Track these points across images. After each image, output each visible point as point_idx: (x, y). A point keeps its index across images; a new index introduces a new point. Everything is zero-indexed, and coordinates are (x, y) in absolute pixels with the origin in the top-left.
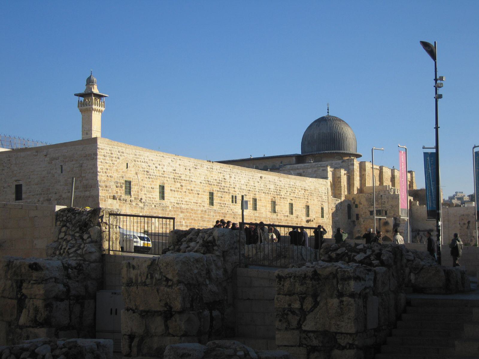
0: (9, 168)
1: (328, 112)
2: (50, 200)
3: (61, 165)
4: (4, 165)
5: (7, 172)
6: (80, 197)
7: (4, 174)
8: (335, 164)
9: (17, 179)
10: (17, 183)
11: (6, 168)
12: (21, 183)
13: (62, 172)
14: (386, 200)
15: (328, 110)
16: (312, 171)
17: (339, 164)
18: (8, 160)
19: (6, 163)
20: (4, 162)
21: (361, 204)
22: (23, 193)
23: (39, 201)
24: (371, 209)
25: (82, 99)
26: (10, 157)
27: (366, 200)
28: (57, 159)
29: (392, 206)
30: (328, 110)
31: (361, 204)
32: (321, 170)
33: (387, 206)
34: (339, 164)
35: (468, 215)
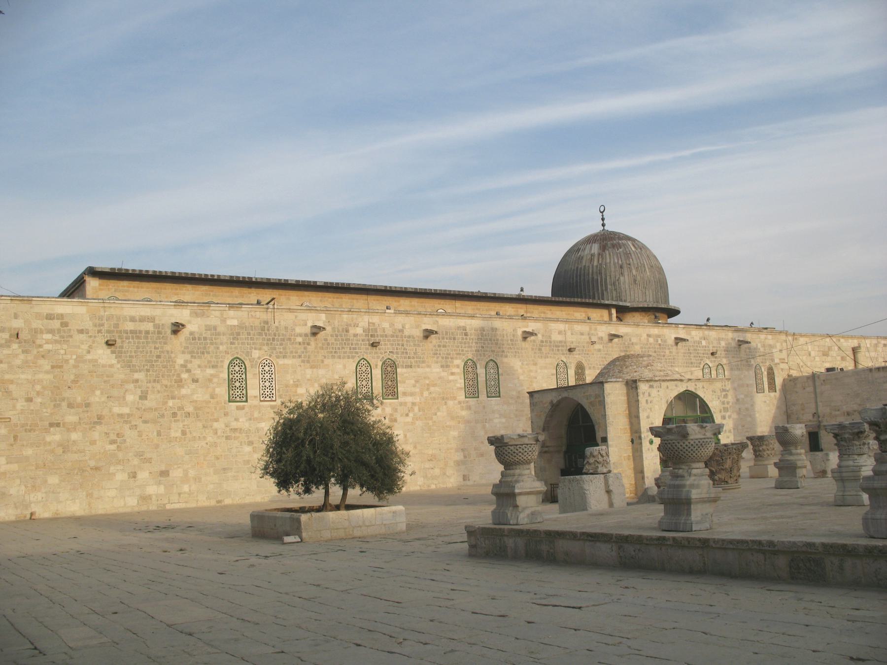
1: (603, 225)
15: (603, 219)
30: (603, 219)
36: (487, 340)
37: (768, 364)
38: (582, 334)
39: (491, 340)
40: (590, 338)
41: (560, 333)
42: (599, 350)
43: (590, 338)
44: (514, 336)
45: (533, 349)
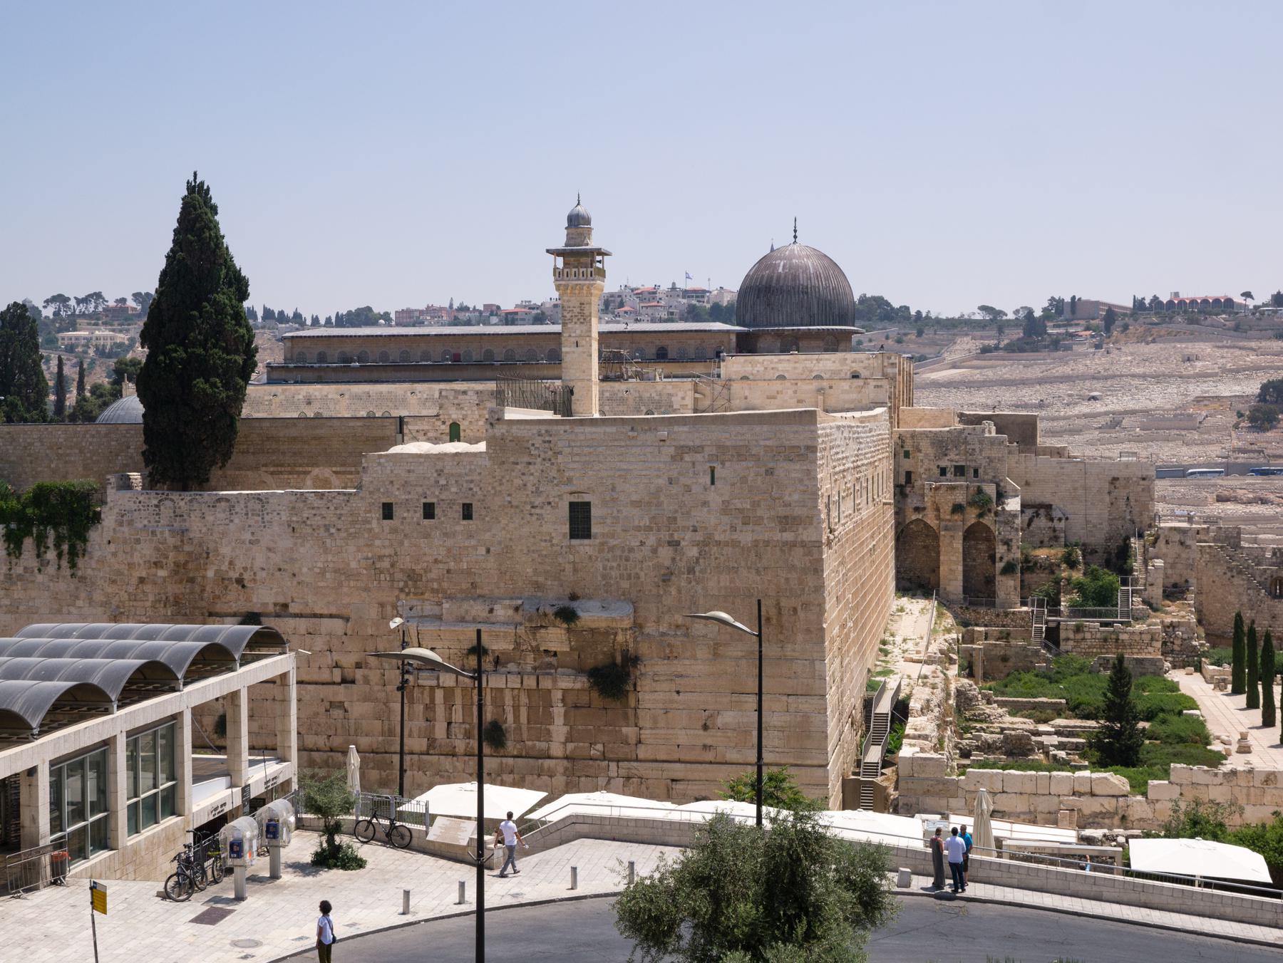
2: (677, 543)
6: (767, 543)
9: (574, 489)
10: (574, 499)
11: (539, 460)
12: (586, 500)
13: (713, 483)
14: (977, 447)
21: (920, 451)
22: (593, 522)
23: (642, 544)
24: (944, 463)
25: (560, 262)
27: (933, 444)
28: (699, 449)
29: (991, 460)
31: (920, 451)
33: (981, 460)
35: (1127, 479)
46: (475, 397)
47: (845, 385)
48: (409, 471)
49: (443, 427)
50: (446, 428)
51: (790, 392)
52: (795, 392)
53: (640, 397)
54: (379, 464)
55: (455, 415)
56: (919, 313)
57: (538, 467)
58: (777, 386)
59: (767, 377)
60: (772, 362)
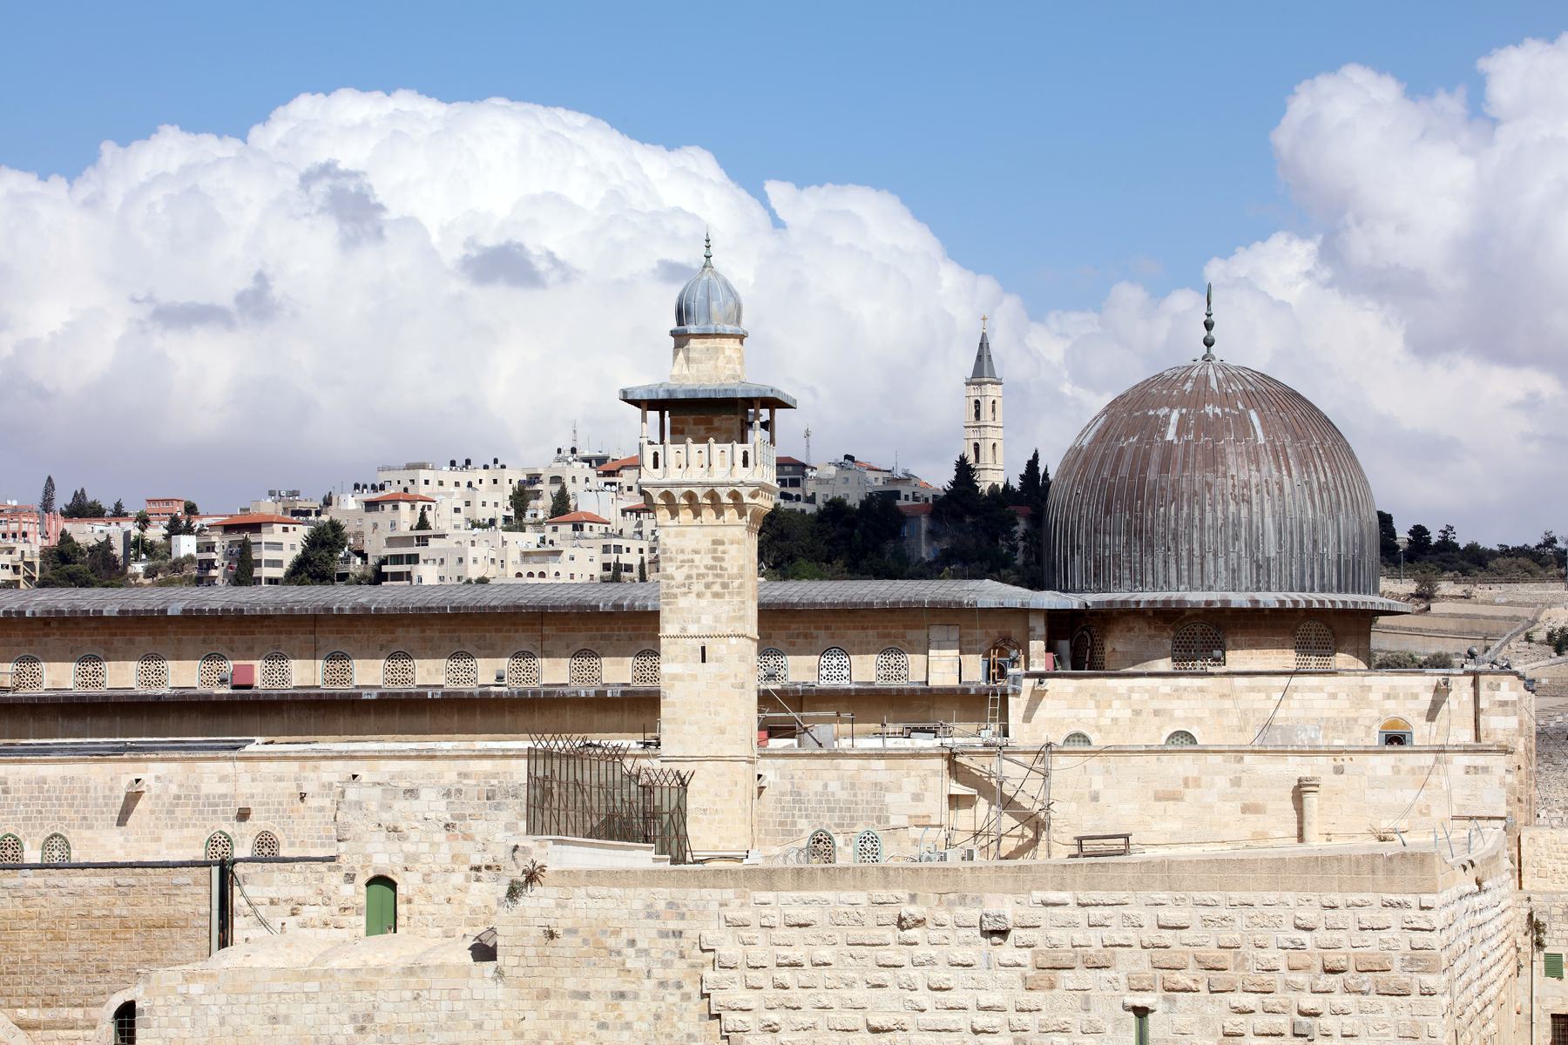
0: (679, 986)
1: (1209, 343)
3: (1141, 1012)
4: (628, 966)
5: (658, 1017)
7: (628, 1026)
8: (1388, 697)
11: (649, 985)
15: (1209, 326)
16: (1396, 770)
17: (1415, 697)
18: (664, 934)
19: (646, 952)
20: (632, 943)
26: (682, 917)
30: (1209, 326)
32: (1461, 772)
34: (1415, 697)
36: (50, 798)
37: (860, 828)
38: (280, 779)
39: (58, 799)
40: (299, 786)
41: (223, 779)
42: (321, 809)
43: (299, 786)
44: (111, 789)
45: (152, 812)
46: (444, 802)
47: (1384, 764)
48: (274, 1019)
49: (348, 890)
50: (356, 893)
51: (1222, 782)
52: (1236, 782)
53: (797, 795)
54: (187, 998)
55: (383, 860)
56: (1419, 532)
57: (646, 1005)
58: (1182, 765)
59: (1141, 740)
60: (1153, 694)
